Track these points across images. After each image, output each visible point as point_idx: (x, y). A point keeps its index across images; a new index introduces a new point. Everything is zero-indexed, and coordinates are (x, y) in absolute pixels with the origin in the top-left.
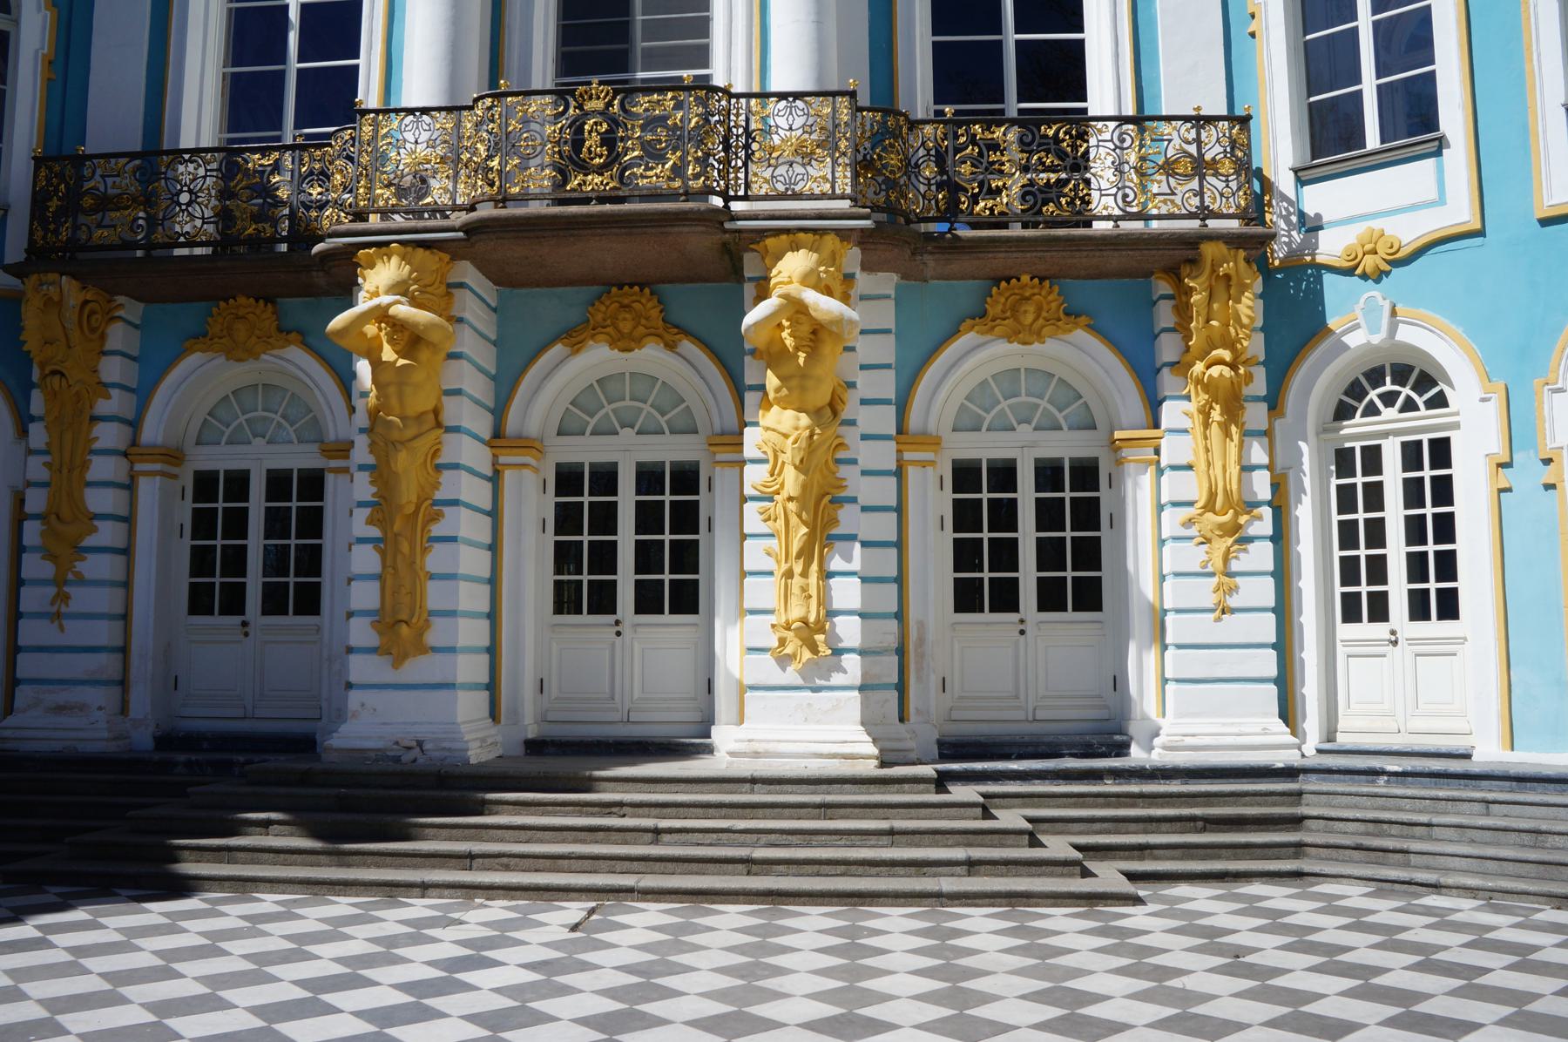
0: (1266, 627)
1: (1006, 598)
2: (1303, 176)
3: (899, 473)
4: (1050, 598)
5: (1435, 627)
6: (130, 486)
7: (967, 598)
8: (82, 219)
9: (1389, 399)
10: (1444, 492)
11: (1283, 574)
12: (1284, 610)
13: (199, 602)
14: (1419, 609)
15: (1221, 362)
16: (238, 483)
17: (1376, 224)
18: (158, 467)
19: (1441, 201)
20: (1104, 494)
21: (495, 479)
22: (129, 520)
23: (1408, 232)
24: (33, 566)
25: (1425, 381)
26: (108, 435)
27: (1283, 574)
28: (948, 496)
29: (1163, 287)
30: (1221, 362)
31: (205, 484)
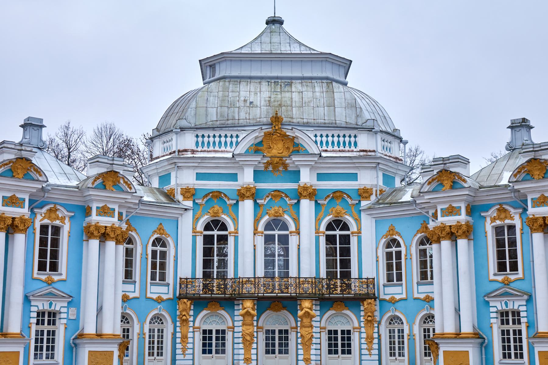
0: (377, 357)
1: (336, 352)
2: (384, 286)
3: (320, 333)
4: (343, 352)
5: (401, 358)
6: (194, 332)
7: (330, 352)
8: (187, 289)
9: (396, 322)
10: (403, 336)
11: (380, 349)
12: (380, 355)
13: (204, 352)
14: (400, 356)
15: (369, 316)
16: (211, 332)
17: (394, 295)
18: (198, 330)
19: (402, 294)
20: (352, 336)
21: (257, 332)
22: (193, 338)
23: (398, 297)
24: (179, 346)
25: (401, 320)
26: (191, 324)
27: (380, 349)
28: (327, 336)
29: (361, 304)
30: (369, 316)
31: (204, 332)
